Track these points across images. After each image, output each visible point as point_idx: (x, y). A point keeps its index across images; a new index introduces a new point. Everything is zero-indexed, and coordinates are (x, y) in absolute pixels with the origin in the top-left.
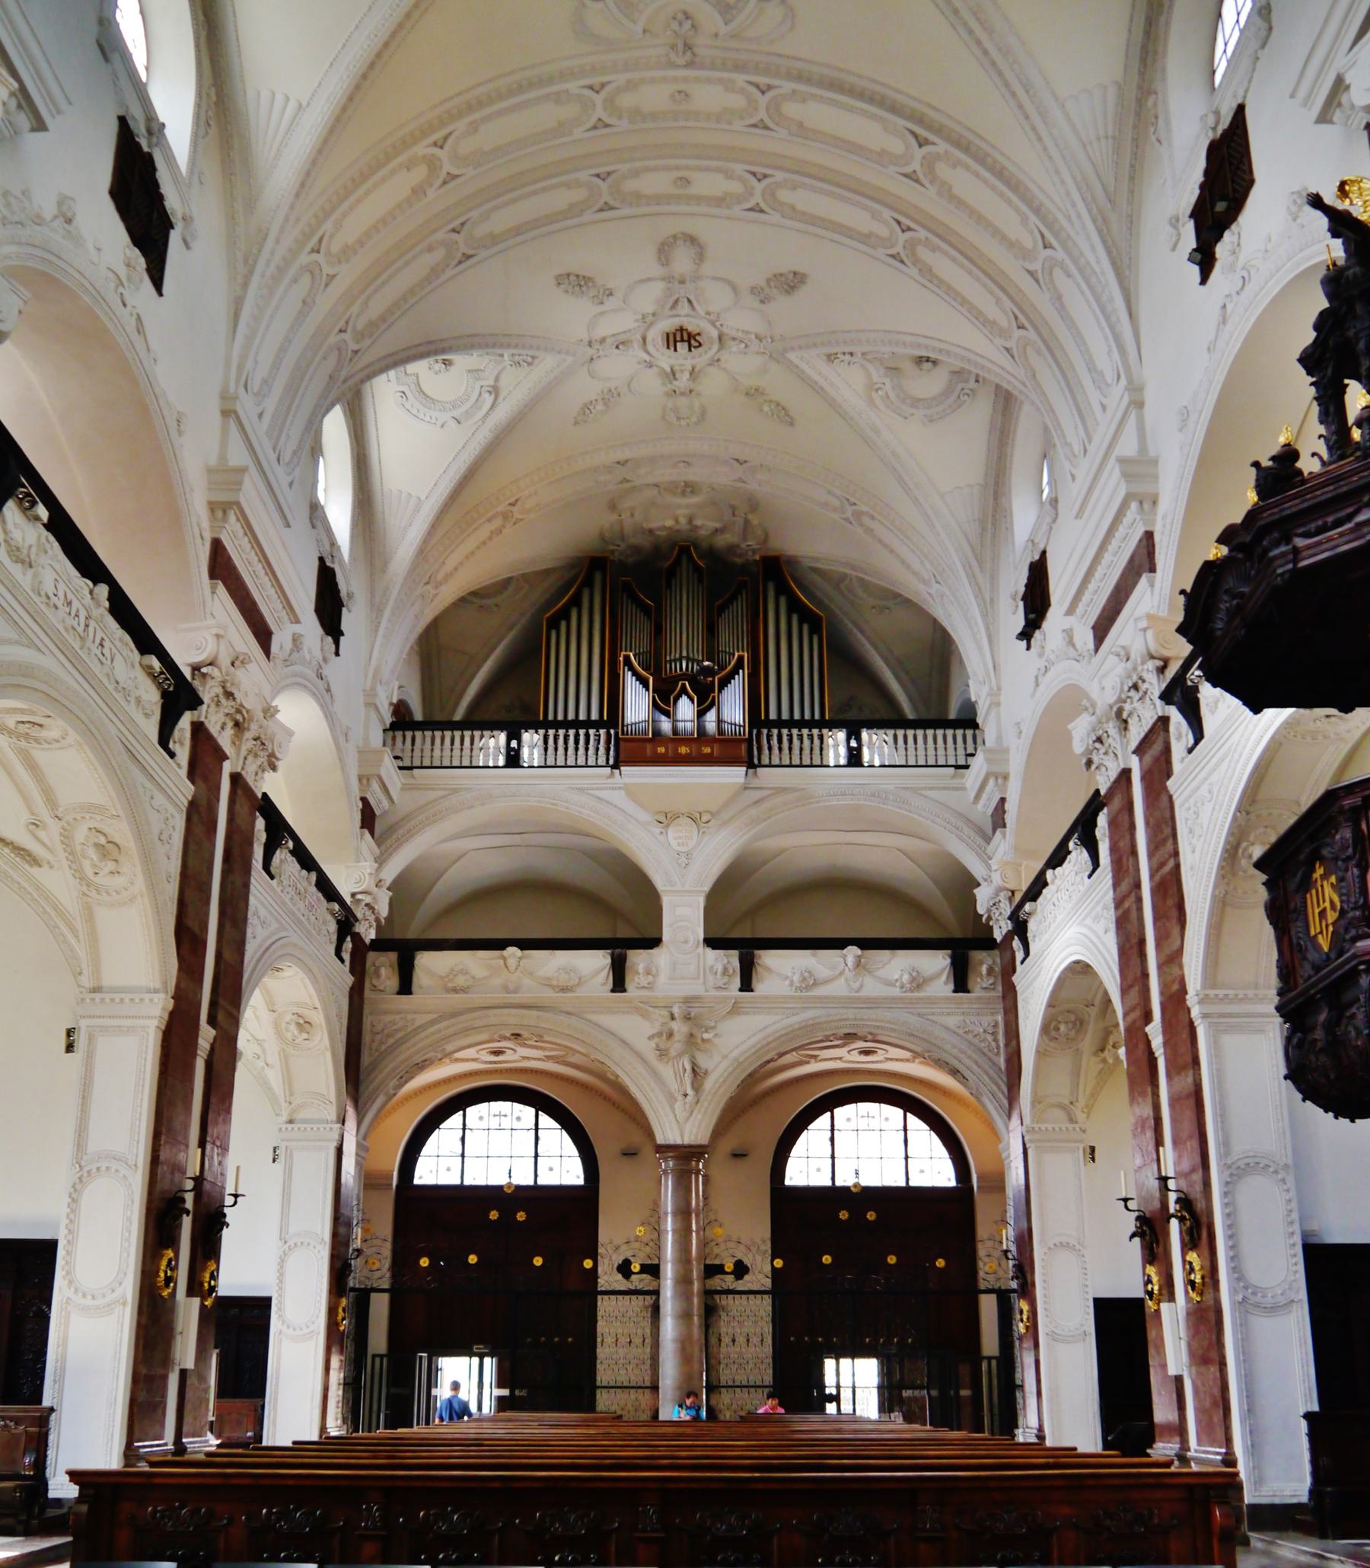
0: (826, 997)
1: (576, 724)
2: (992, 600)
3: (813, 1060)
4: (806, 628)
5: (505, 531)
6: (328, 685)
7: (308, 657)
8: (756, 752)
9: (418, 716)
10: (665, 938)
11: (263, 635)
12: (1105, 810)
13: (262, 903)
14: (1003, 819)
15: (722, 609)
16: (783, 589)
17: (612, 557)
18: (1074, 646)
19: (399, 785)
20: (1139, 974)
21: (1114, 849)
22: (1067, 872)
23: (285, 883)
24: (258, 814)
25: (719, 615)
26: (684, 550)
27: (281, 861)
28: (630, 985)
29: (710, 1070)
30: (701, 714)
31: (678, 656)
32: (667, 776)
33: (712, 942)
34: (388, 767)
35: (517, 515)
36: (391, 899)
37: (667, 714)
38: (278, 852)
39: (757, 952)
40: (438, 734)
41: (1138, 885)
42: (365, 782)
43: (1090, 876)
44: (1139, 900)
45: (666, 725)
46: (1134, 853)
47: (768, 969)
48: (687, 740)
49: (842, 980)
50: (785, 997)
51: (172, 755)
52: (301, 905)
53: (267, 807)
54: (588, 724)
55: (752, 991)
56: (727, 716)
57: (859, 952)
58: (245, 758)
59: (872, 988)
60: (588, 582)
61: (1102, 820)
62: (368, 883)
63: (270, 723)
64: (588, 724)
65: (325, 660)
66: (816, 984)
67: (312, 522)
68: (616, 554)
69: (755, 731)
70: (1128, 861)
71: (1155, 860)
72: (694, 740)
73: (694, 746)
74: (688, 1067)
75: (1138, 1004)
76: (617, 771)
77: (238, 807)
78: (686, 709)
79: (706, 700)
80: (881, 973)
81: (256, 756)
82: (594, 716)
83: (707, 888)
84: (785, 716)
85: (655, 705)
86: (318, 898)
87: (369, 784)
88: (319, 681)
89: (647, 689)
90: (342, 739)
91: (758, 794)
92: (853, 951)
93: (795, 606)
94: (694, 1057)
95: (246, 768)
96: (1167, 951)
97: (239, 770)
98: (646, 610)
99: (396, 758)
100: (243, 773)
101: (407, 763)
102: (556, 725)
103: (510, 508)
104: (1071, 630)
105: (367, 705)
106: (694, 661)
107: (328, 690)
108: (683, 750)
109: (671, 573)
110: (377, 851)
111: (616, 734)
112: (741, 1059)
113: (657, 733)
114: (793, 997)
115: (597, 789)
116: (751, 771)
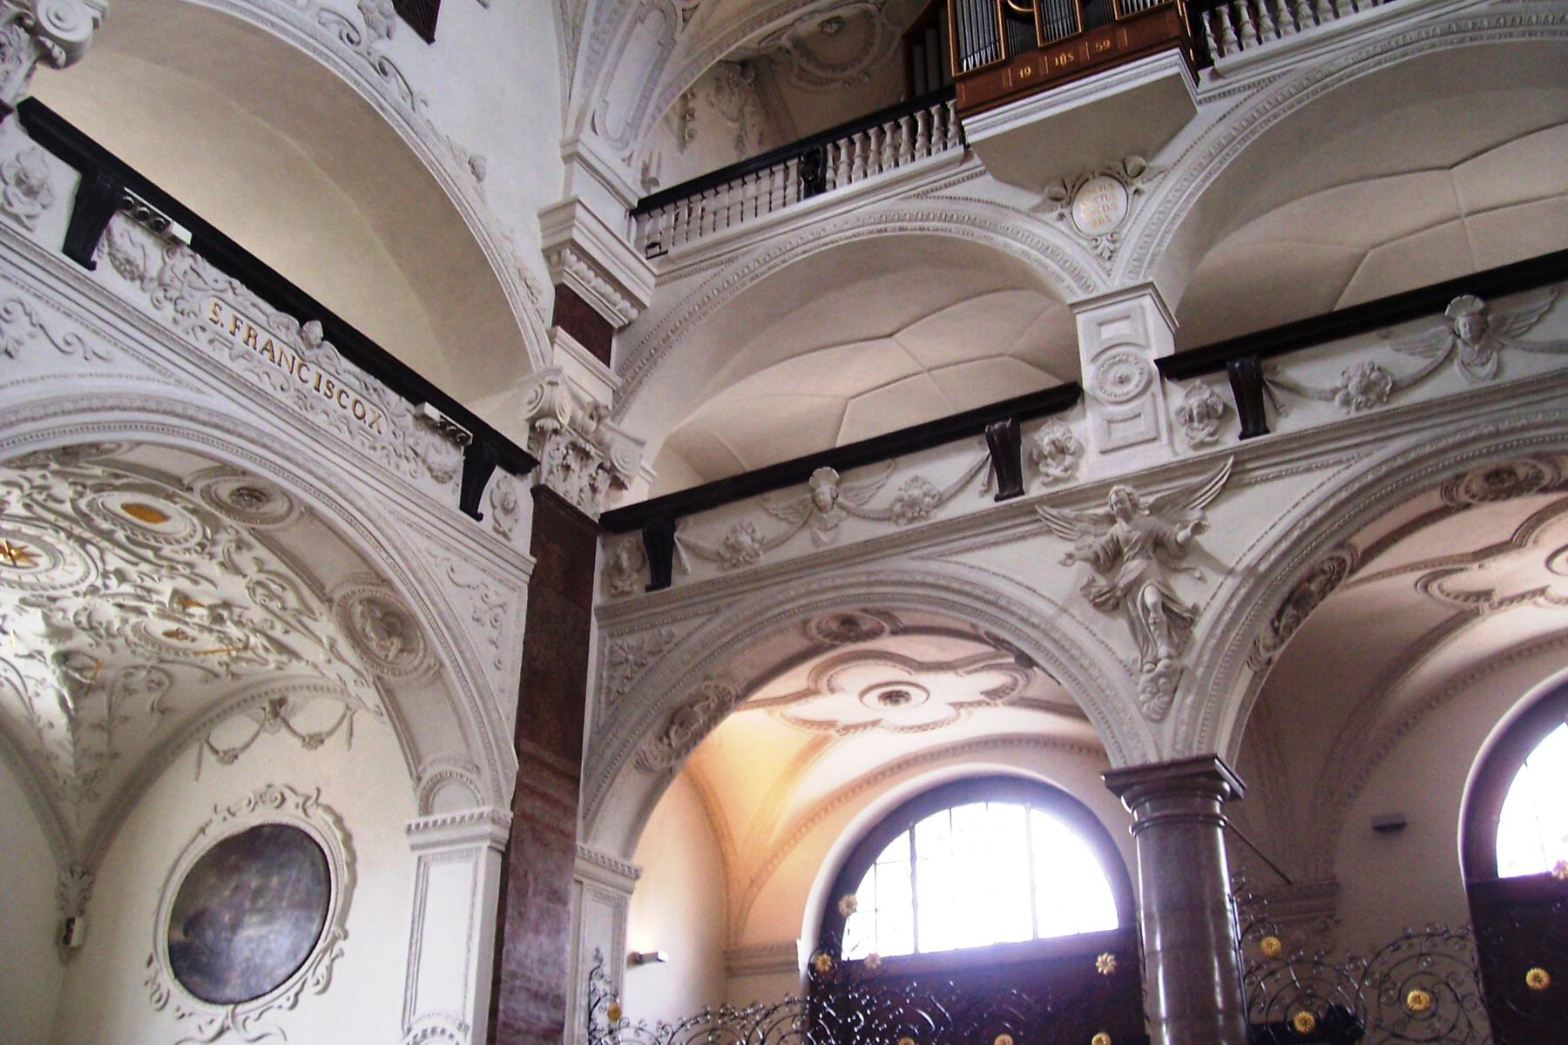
3: (1485, 606)
10: (1086, 384)
19: (652, 281)
29: (1202, 605)
33: (1174, 368)
39: (1266, 363)
42: (554, 258)
47: (1295, 390)
49: (1455, 368)
57: (1479, 304)
59: (1519, 365)
66: (1398, 388)
72: (1080, 36)
87: (562, 261)
94: (1168, 587)
105: (568, 159)
108: (1062, 59)
110: (618, 381)
112: (1262, 568)
115: (946, 186)
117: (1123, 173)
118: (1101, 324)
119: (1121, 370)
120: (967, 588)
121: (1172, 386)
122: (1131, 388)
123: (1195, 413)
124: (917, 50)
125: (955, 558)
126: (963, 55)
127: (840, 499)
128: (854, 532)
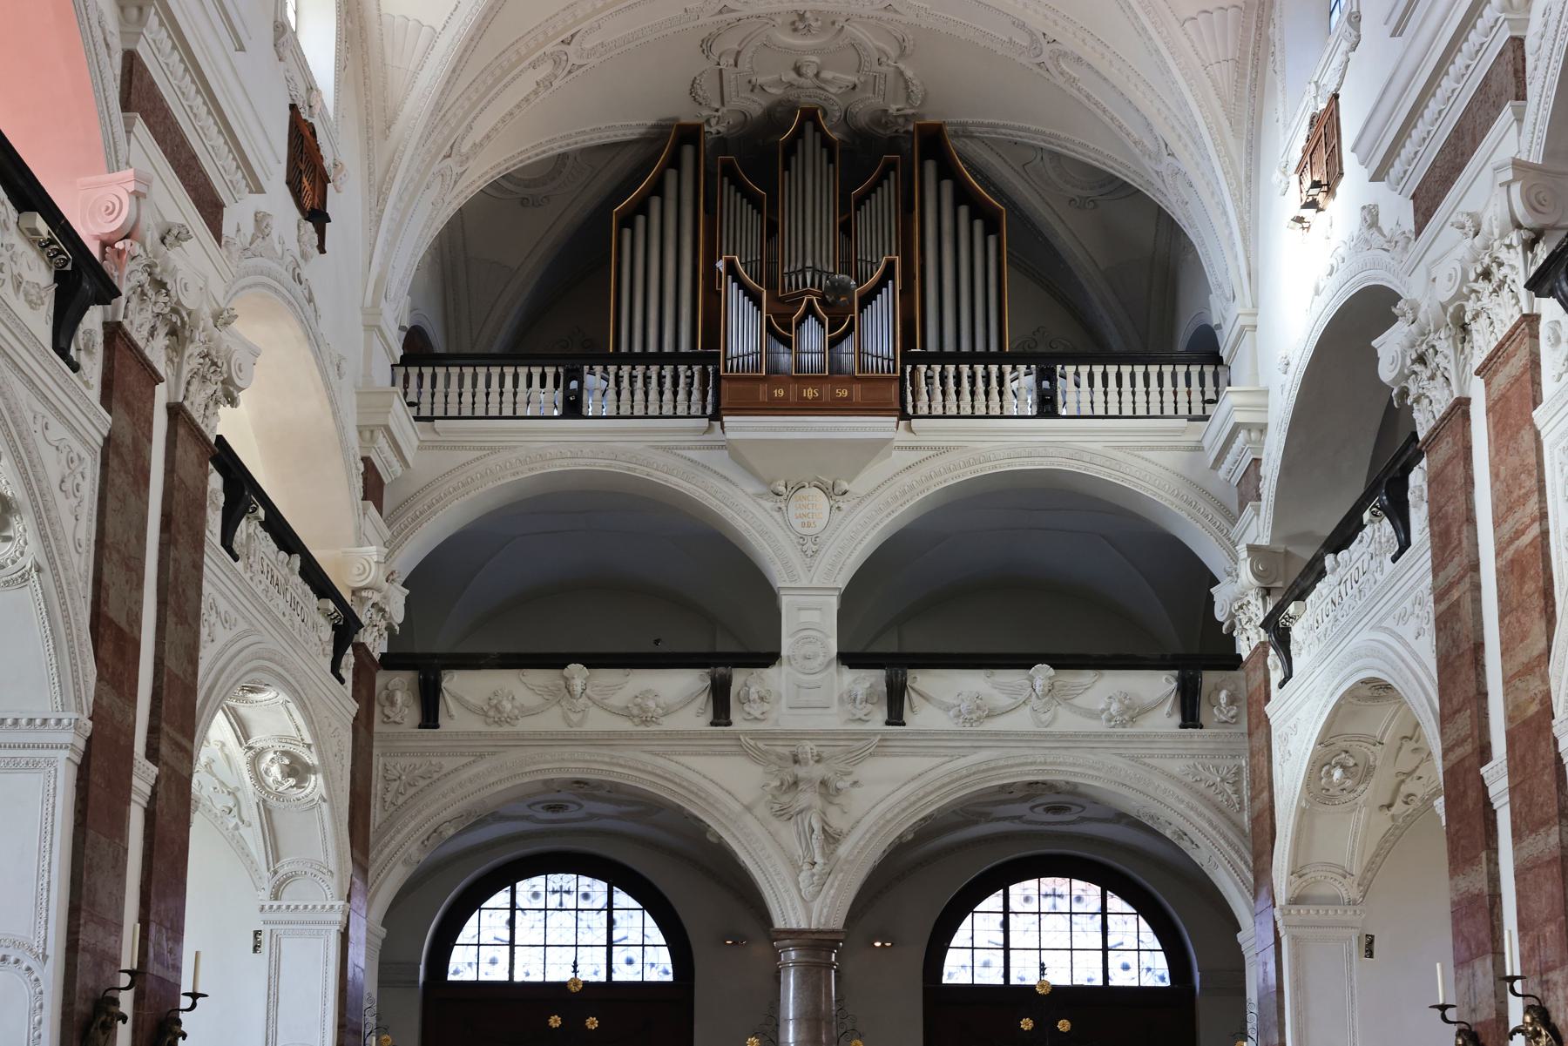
0: (1007, 733)
1: (661, 358)
2: (1248, 179)
4: (978, 224)
5: (556, 84)
6: (310, 293)
7: (278, 248)
8: (910, 398)
9: (439, 346)
10: (784, 653)
11: (211, 208)
12: (1424, 463)
13: (222, 594)
14: (1257, 488)
15: (860, 201)
16: (946, 170)
17: (706, 128)
18: (1380, 230)
20: (1472, 692)
21: (1434, 518)
22: (1355, 557)
23: (256, 567)
24: (211, 466)
25: (858, 208)
26: (810, 115)
27: (249, 536)
28: (735, 715)
30: (834, 343)
31: (800, 266)
32: (787, 429)
33: (849, 659)
34: (399, 416)
35: (574, 59)
36: (407, 598)
37: (787, 342)
38: (243, 522)
39: (911, 673)
40: (468, 371)
41: (1475, 567)
43: (1394, 559)
44: (1477, 587)
45: (785, 359)
46: (1471, 520)
48: (815, 380)
49: (1027, 710)
50: (948, 733)
51: (75, 367)
52: (280, 600)
53: (224, 457)
54: (676, 358)
55: (904, 724)
56: (870, 347)
57: (1052, 672)
58: (189, 383)
60: (675, 162)
61: (1417, 479)
62: (374, 575)
63: (223, 334)
64: (676, 358)
65: (304, 255)
67: (278, 53)
68: (713, 122)
69: (909, 368)
70: (1459, 532)
71: (1506, 528)
73: (827, 388)
74: (817, 826)
75: (1471, 735)
76: (717, 424)
77: (179, 452)
78: (812, 337)
79: (841, 325)
80: (1078, 701)
81: (204, 379)
82: (685, 347)
83: (842, 583)
84: (949, 347)
85: (770, 329)
86: (304, 592)
88: (297, 285)
89: (760, 308)
90: (332, 372)
91: (913, 457)
92: (1043, 672)
93: (963, 195)
95: (191, 398)
96: (1522, 657)
97: (180, 400)
98: (754, 201)
99: (410, 404)
100: (186, 404)
101: (425, 412)
102: (632, 359)
103: (564, 48)
104: (1375, 206)
106: (821, 272)
107: (310, 300)
108: (809, 393)
109: (791, 148)
111: (717, 371)
113: (773, 370)
114: (960, 733)
116: (902, 423)
117: (831, 489)
118: (799, 609)
119: (808, 649)
120: (685, 784)
121: (845, 669)
122: (815, 664)
123: (859, 697)
124: (627, 232)
125: (676, 758)
126: (729, 356)
127: (588, 691)
128: (598, 721)
